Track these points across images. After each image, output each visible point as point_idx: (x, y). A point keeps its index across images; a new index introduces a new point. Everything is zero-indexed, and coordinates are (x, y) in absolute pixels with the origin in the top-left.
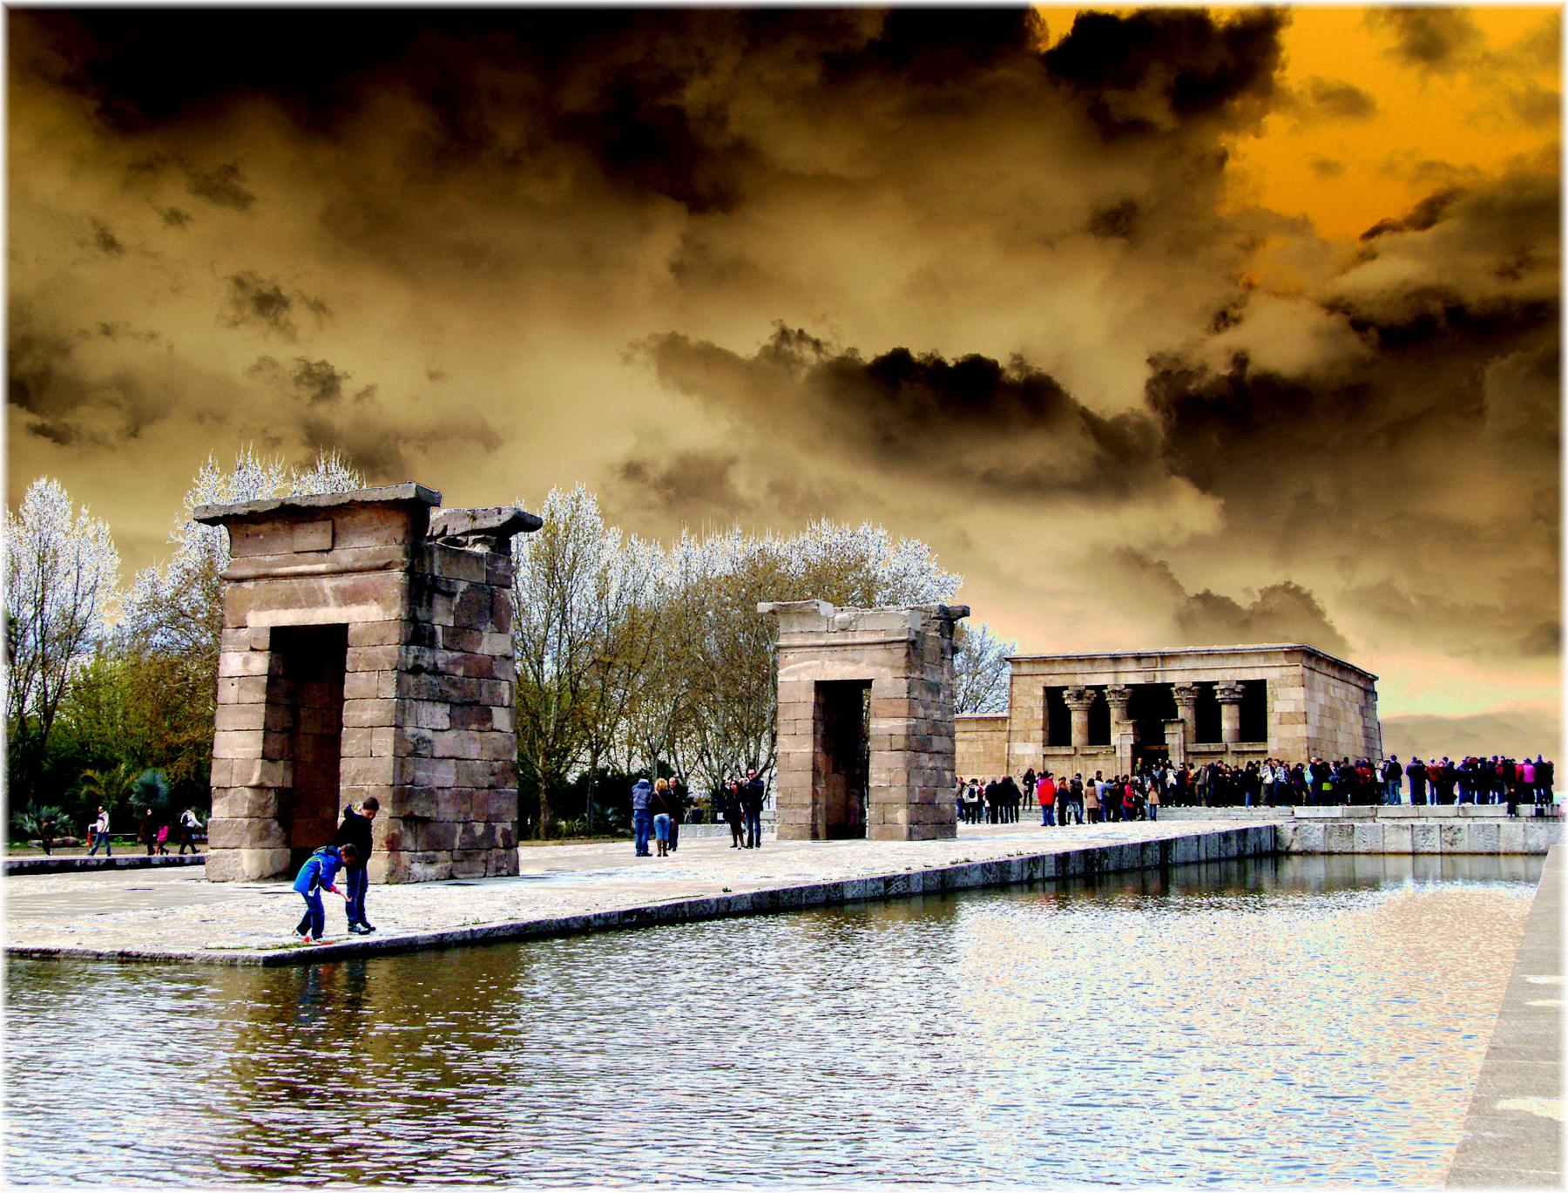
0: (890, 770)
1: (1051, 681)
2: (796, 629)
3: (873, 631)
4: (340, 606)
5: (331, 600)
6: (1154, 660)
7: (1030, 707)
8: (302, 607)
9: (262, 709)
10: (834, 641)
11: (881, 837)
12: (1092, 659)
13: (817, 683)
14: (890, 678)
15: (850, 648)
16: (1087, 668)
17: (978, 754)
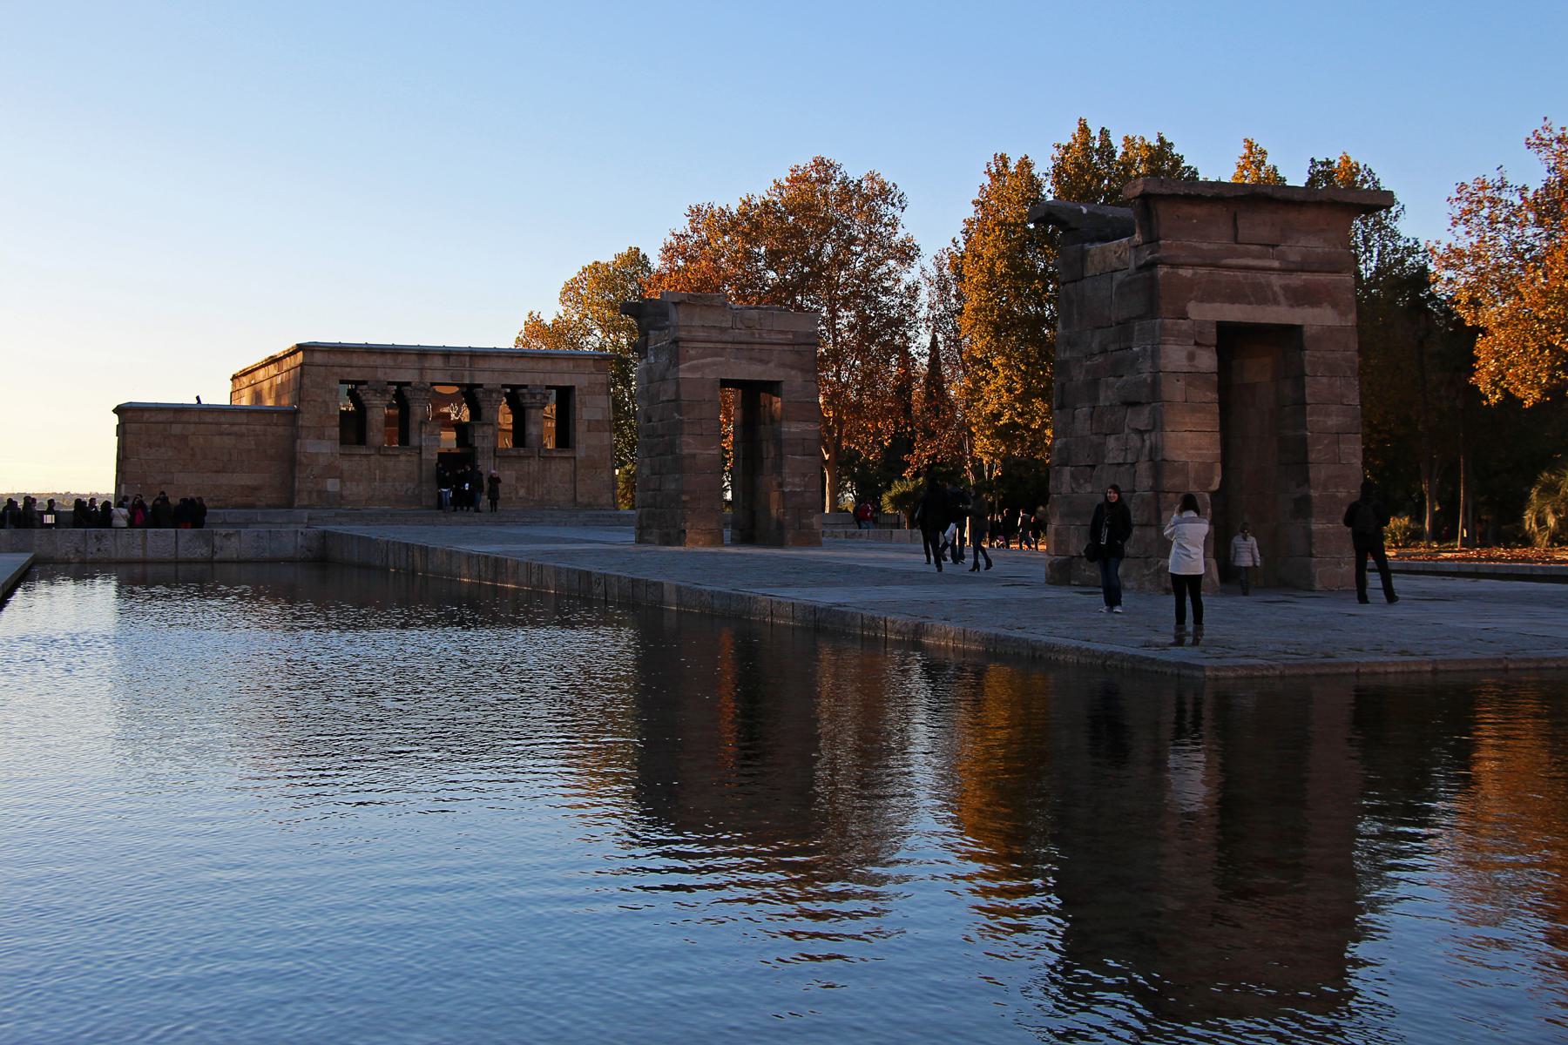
0: (804, 475)
1: (349, 374)
2: (696, 322)
3: (781, 332)
4: (1292, 306)
5: (1282, 299)
6: (463, 358)
7: (325, 401)
8: (1250, 303)
13: (722, 380)
14: (800, 380)
15: (757, 347)
16: (389, 361)
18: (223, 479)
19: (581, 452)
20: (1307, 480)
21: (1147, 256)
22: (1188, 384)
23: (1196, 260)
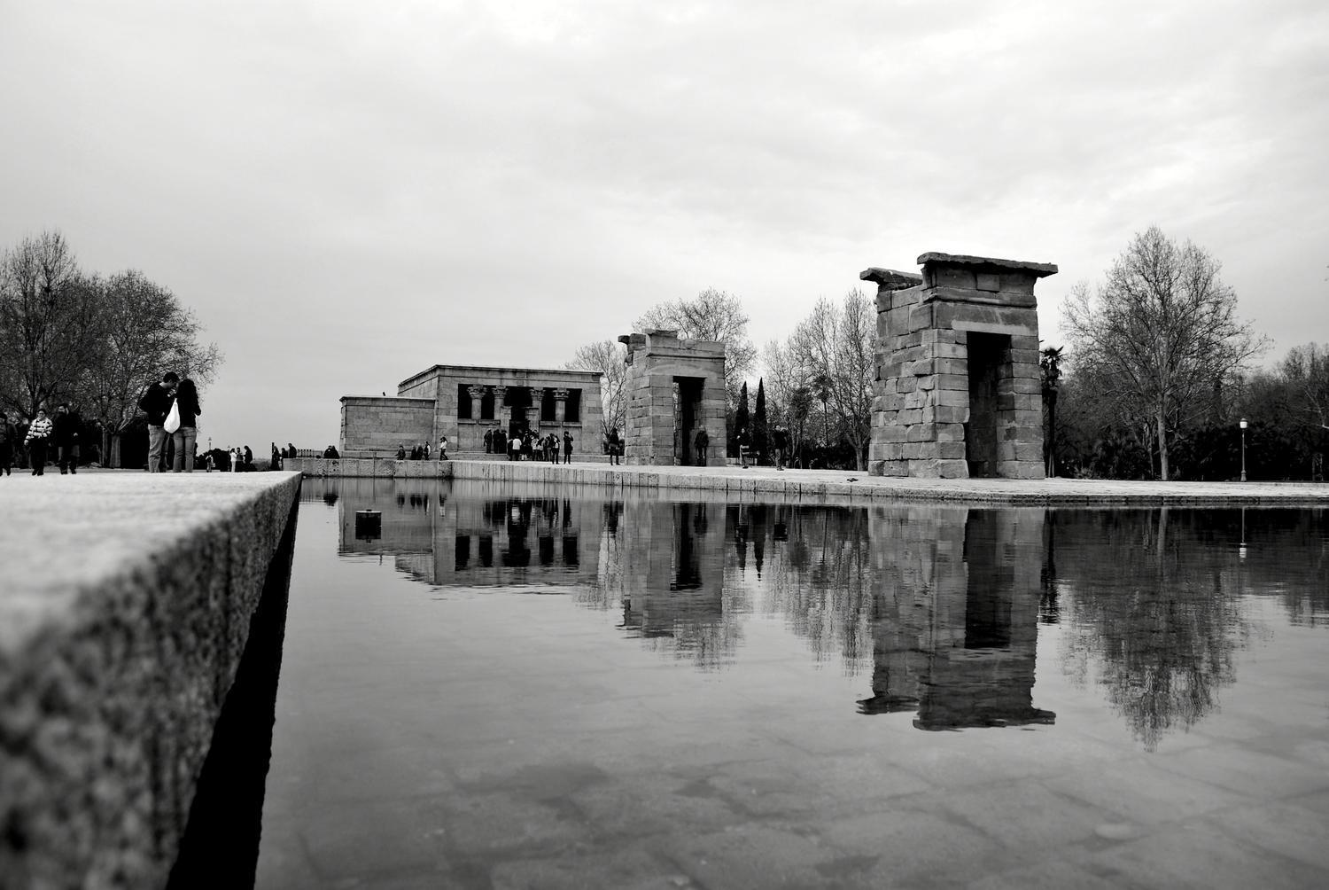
0: (717, 428)
3: (706, 351)
5: (1000, 320)
9: (967, 378)
10: (684, 355)
11: (713, 465)
12: (488, 370)
13: (674, 377)
14: (716, 377)
16: (485, 375)
17: (410, 421)
18: (396, 436)
19: (585, 424)
20: (1014, 419)
21: (929, 295)
22: (952, 365)
23: (957, 297)
